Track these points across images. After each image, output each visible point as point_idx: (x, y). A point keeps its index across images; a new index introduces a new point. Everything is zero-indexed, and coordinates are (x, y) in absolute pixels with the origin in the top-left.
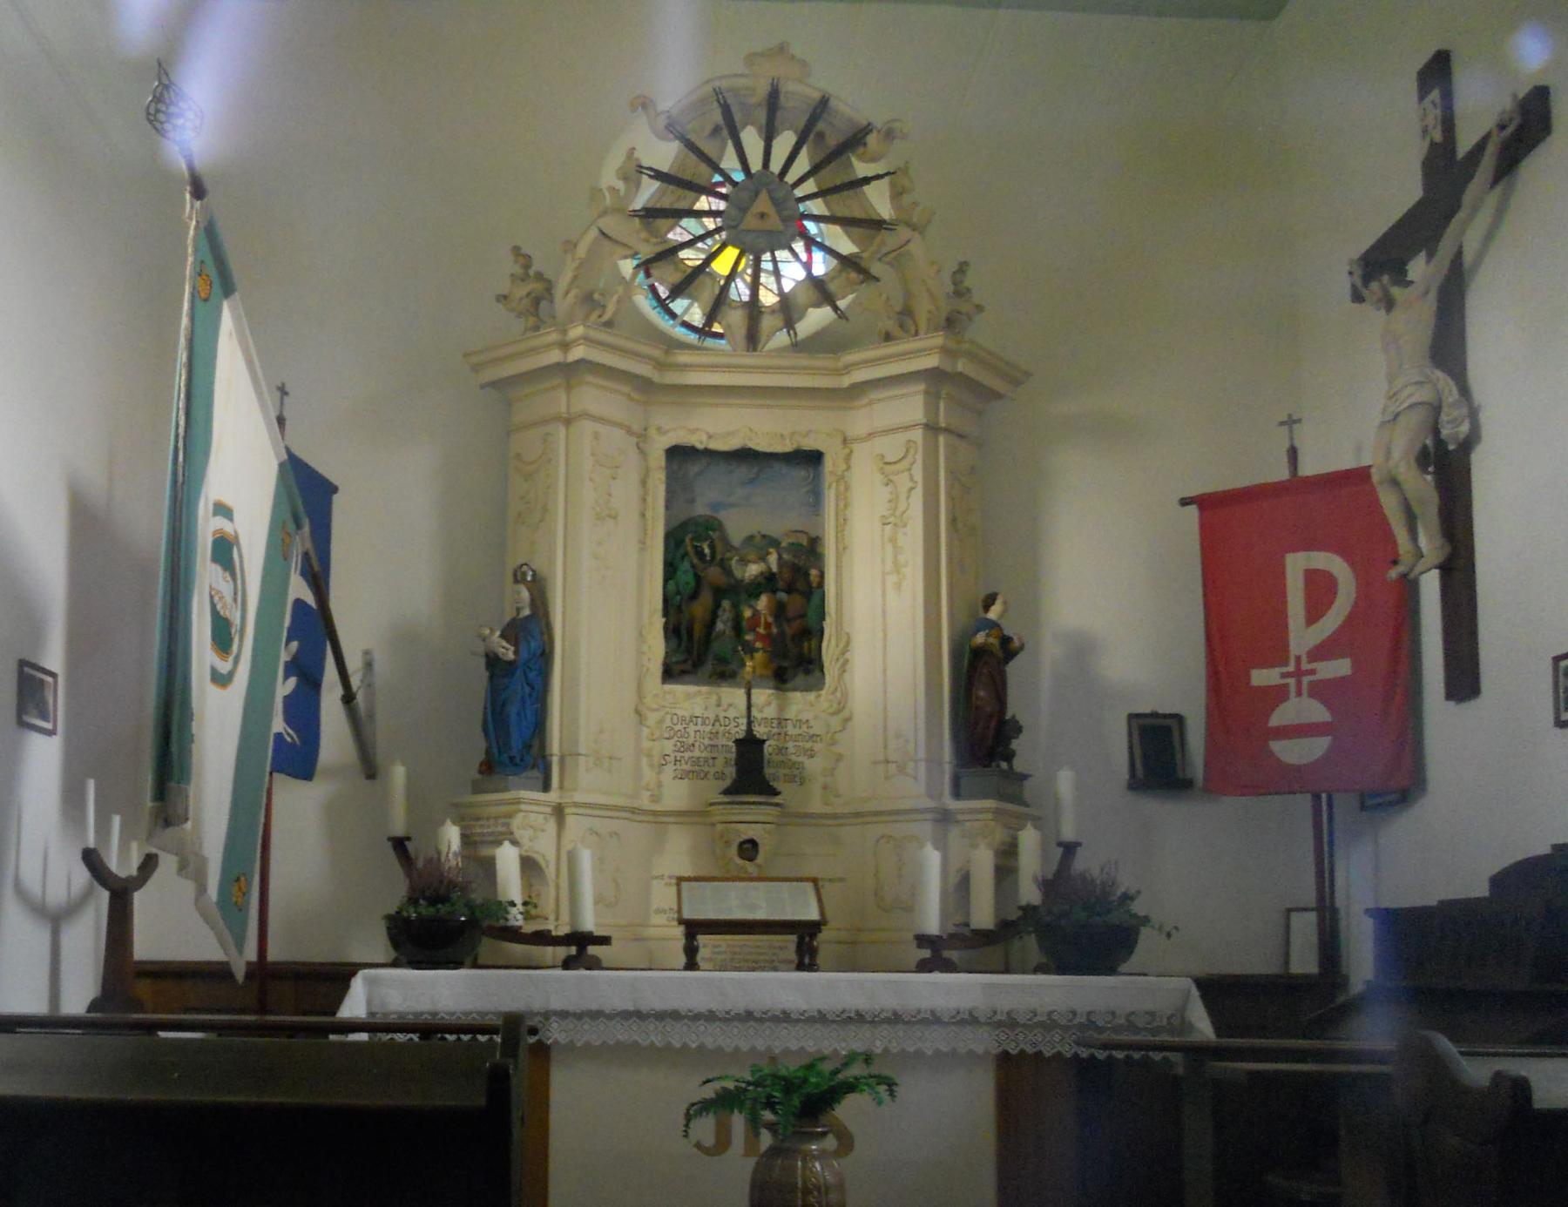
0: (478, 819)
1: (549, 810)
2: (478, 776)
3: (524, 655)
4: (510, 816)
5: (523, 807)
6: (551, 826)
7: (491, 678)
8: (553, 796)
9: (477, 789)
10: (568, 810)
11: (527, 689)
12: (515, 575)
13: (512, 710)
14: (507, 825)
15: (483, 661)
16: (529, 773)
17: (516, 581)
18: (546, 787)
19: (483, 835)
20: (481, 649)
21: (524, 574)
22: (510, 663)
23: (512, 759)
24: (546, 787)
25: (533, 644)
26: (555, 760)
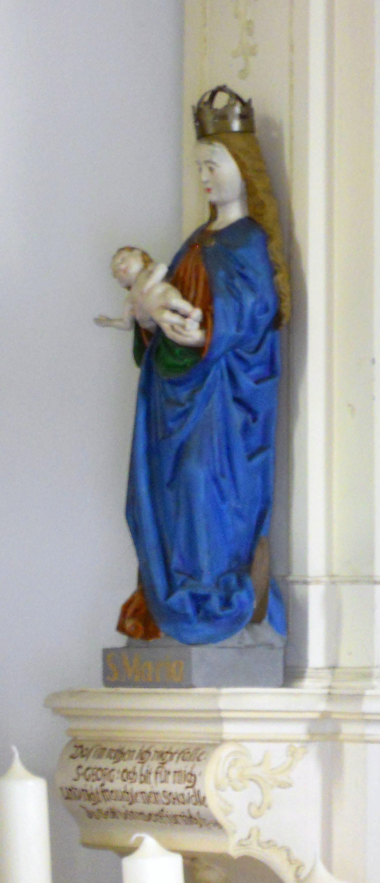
0: (119, 754)
1: (299, 730)
2: (120, 640)
3: (227, 329)
4: (196, 753)
5: (229, 730)
6: (308, 771)
7: (146, 390)
8: (308, 695)
9: (116, 671)
10: (348, 729)
11: (238, 417)
12: (199, 115)
13: (198, 472)
14: (191, 778)
15: (127, 340)
16: (244, 636)
17: (203, 134)
18: (291, 673)
19: (131, 798)
20: (120, 310)
21: (223, 116)
22: (195, 351)
23: (199, 601)
24: (291, 673)
25: (249, 300)
26: (315, 602)
